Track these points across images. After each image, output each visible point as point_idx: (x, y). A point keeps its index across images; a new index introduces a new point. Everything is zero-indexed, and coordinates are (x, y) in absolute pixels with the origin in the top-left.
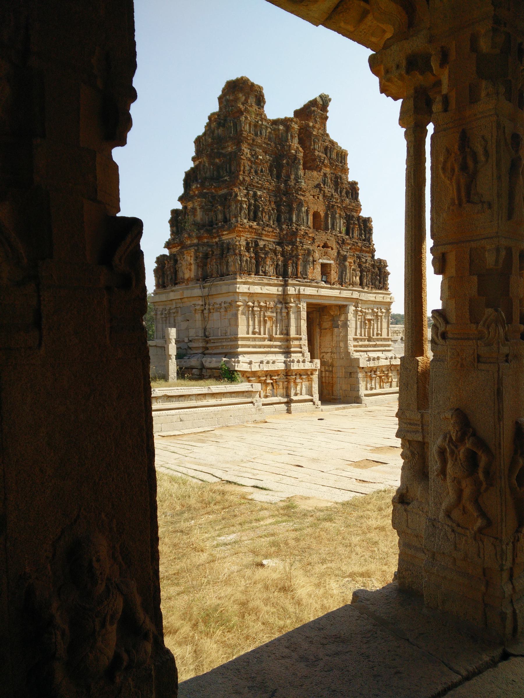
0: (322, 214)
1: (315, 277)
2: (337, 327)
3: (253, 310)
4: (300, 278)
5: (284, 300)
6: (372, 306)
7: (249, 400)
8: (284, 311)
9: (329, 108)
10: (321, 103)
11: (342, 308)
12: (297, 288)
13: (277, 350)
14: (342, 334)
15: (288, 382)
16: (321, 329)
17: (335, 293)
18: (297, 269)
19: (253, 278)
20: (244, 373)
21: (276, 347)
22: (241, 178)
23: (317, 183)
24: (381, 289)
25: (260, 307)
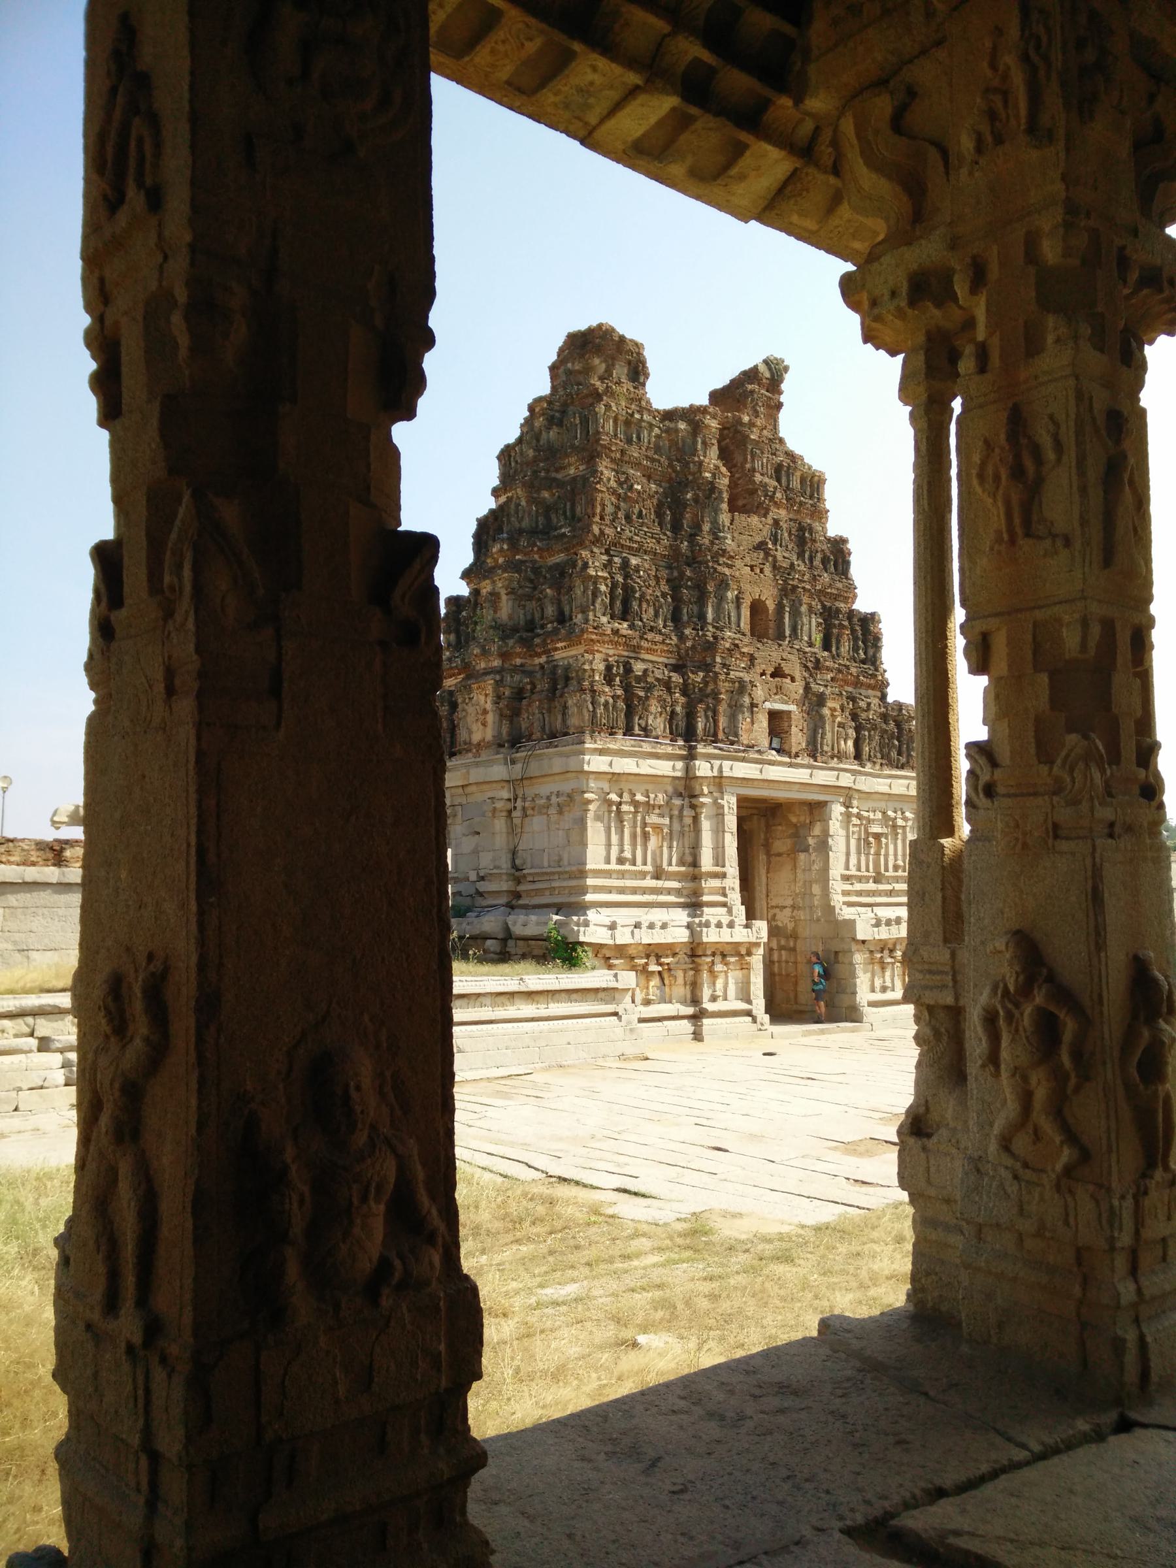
0: (771, 605)
1: (755, 739)
2: (806, 850)
3: (619, 811)
4: (722, 741)
5: (687, 790)
6: (882, 805)
7: (610, 1008)
8: (688, 812)
9: (783, 386)
10: (768, 375)
11: (816, 809)
12: (717, 763)
13: (672, 899)
14: (816, 867)
15: (697, 970)
16: (768, 854)
17: (800, 775)
18: (716, 722)
19: (621, 742)
20: (598, 948)
21: (669, 891)
22: (596, 530)
23: (758, 539)
24: (902, 767)
25: (636, 804)
